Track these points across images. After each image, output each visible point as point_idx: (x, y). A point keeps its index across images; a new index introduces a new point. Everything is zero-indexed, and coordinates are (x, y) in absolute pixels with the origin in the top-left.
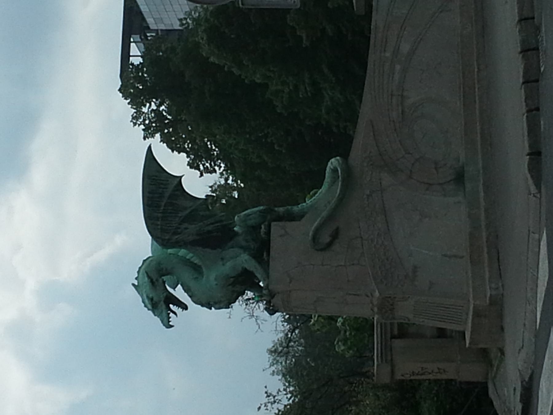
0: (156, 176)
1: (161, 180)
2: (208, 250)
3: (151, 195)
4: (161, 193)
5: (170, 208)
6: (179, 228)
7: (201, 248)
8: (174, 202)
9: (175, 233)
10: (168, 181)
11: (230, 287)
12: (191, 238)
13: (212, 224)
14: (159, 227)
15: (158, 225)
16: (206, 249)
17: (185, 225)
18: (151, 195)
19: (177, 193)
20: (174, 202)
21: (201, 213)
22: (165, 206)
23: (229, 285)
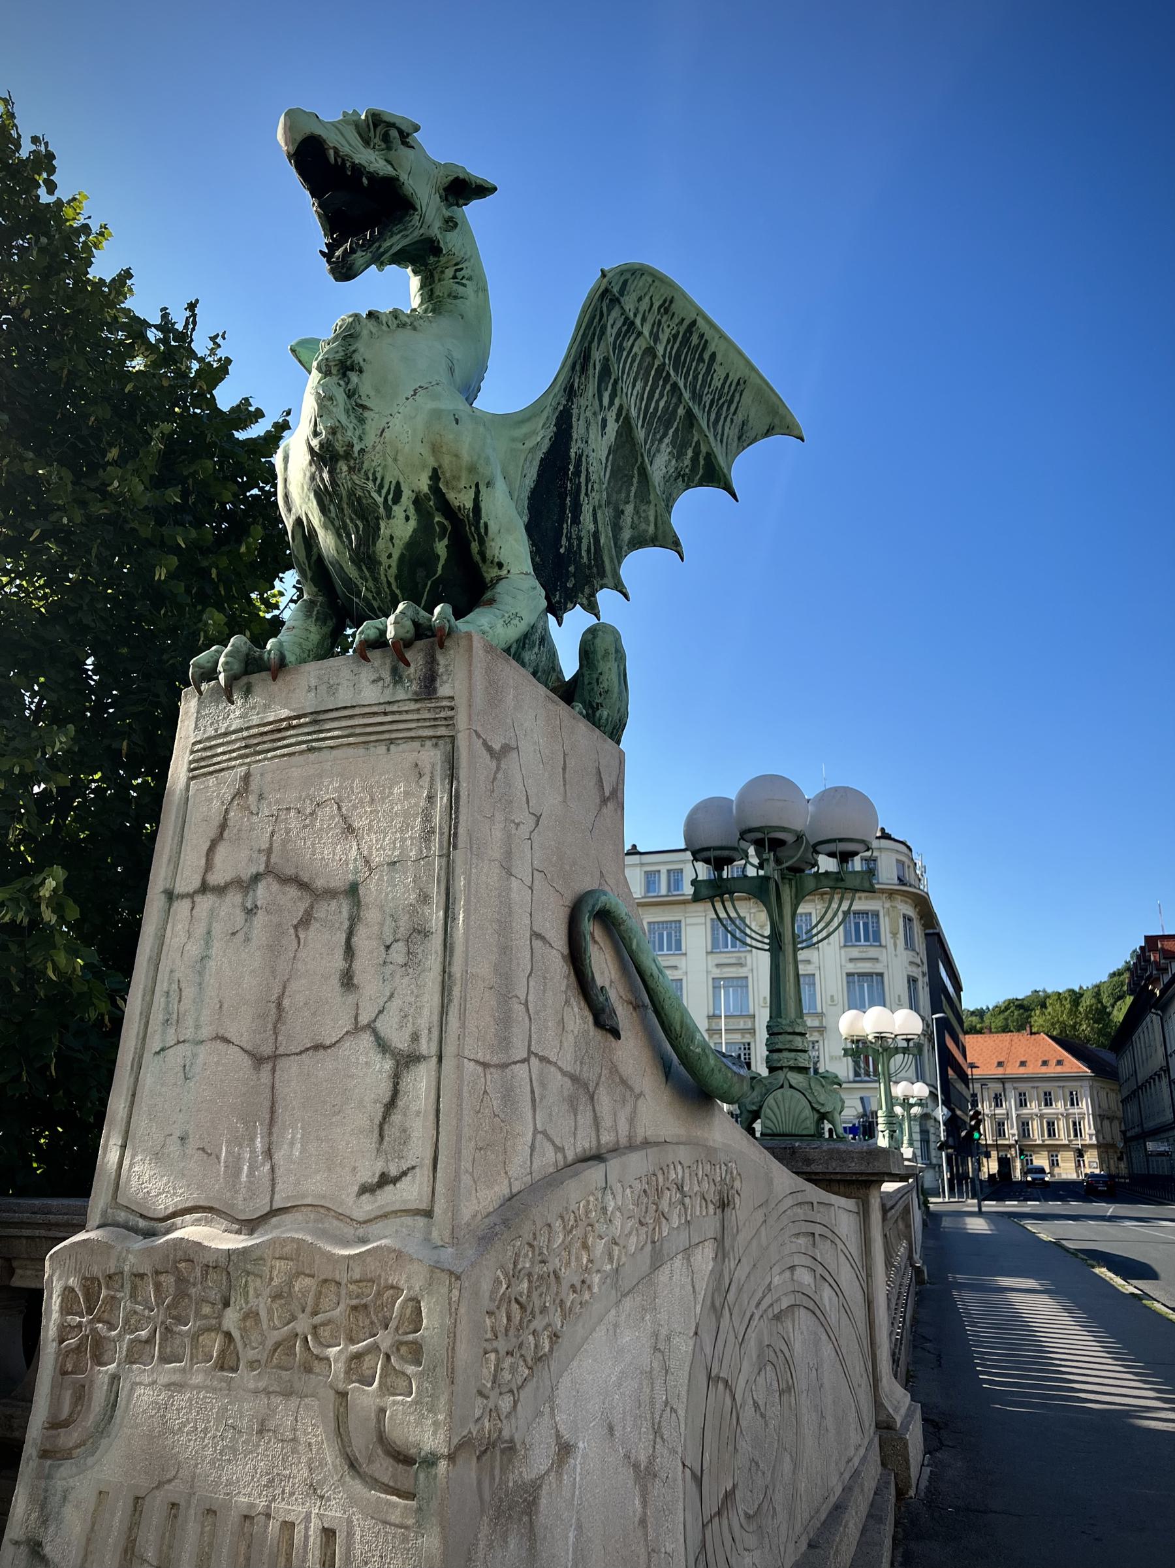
0: (734, 414)
1: (725, 419)
2: (533, 473)
3: (706, 357)
4: (701, 397)
5: (662, 404)
6: (611, 403)
7: (545, 446)
8: (671, 432)
9: (606, 371)
10: (721, 441)
11: (423, 484)
12: (578, 430)
13: (596, 535)
14: (638, 322)
15: (644, 320)
16: (536, 463)
17: (612, 427)
18: (706, 357)
19: (690, 453)
20: (671, 432)
21: (629, 509)
22: (675, 386)
23: (435, 476)
